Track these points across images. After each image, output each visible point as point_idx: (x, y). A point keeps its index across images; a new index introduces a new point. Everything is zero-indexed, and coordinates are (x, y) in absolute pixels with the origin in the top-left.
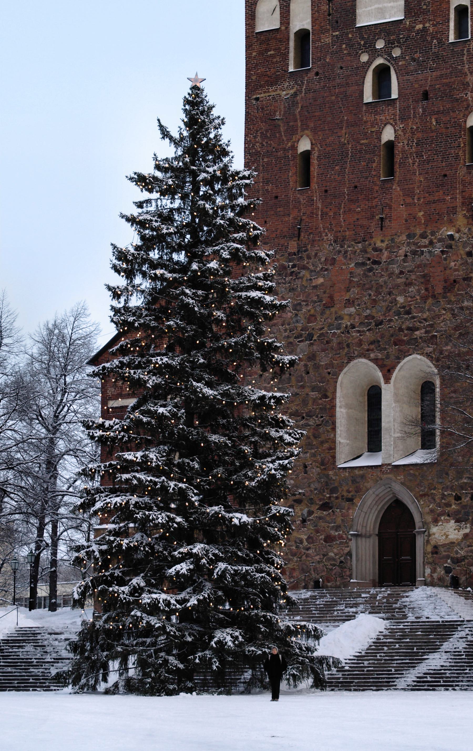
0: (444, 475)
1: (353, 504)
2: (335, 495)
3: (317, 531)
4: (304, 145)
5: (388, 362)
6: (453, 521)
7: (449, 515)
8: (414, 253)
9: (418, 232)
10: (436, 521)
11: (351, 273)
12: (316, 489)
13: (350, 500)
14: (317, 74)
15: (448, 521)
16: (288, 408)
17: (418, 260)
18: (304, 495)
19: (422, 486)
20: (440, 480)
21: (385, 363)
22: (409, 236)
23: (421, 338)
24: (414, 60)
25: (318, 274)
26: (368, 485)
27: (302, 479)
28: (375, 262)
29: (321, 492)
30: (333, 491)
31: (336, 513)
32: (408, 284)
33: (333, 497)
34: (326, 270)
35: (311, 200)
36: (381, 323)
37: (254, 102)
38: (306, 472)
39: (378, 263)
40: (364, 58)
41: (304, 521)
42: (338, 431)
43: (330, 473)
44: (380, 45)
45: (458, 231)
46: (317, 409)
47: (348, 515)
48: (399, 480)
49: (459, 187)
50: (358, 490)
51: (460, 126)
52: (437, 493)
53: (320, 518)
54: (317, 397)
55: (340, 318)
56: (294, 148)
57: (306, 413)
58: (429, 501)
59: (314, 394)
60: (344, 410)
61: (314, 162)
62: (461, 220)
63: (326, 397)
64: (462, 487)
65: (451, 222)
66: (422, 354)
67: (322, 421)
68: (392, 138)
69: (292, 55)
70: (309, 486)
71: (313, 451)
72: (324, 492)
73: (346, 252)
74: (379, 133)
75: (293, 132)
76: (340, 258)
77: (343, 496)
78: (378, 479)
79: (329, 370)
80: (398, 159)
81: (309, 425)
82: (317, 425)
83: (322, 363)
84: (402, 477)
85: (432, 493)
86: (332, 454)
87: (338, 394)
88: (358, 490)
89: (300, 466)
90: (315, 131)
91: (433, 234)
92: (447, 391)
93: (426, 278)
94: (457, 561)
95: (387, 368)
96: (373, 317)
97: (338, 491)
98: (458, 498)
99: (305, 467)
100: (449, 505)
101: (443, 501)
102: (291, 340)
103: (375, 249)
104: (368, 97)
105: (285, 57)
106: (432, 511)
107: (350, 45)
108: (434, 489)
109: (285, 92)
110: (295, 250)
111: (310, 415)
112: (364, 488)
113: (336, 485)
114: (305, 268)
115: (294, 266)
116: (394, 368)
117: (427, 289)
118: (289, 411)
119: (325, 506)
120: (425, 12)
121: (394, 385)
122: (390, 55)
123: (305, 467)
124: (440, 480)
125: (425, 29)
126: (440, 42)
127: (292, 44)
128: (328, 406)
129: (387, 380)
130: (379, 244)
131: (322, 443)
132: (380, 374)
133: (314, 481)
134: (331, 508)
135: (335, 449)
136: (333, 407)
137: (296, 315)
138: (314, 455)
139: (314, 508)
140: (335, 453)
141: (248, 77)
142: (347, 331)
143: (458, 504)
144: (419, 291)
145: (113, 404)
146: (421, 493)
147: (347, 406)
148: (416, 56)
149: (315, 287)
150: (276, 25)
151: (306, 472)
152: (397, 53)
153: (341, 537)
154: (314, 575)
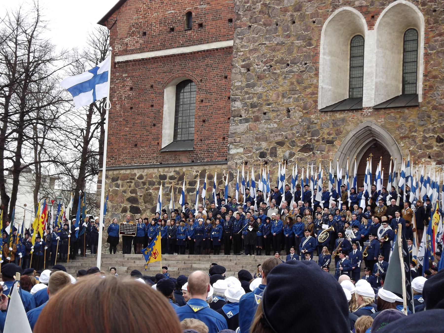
0: (426, 118)
1: (333, 146)
2: (316, 138)
6: (434, 163)
7: (430, 157)
12: (297, 132)
13: (331, 142)
15: (428, 163)
16: (274, 56)
18: (286, 138)
19: (402, 129)
20: (422, 123)
21: (369, 10)
26: (348, 128)
27: (285, 122)
31: (317, 155)
33: (314, 139)
38: (289, 116)
42: (320, 76)
43: (312, 116)
46: (301, 56)
47: (328, 157)
48: (380, 122)
50: (339, 133)
52: (419, 136)
54: (301, 45)
57: (291, 60)
58: (409, 143)
59: (298, 43)
60: (328, 58)
63: (310, 45)
67: (306, 68)
70: (292, 130)
71: (296, 96)
72: (305, 135)
77: (323, 139)
78: (359, 122)
79: (314, 19)
81: (293, 72)
82: (301, 72)
83: (308, 13)
84: (383, 120)
85: (413, 136)
86: (314, 99)
87: (322, 42)
88: (339, 133)
89: (283, 110)
92: (431, 34)
95: (370, 15)
97: (319, 134)
99: (289, 111)
100: (430, 147)
101: (424, 143)
108: (415, 131)
112: (344, 131)
113: (317, 128)
116: (378, 14)
118: (275, 59)
119: (306, 148)
121: (378, 31)
123: (289, 111)
124: (422, 123)
128: (312, 54)
129: (371, 25)
131: (305, 88)
133: (296, 125)
134: (312, 150)
135: (317, 94)
136: (317, 54)
139: (295, 150)
140: (317, 97)
143: (440, 146)
145: (119, 59)
146: (401, 135)
147: (331, 54)
151: (289, 116)
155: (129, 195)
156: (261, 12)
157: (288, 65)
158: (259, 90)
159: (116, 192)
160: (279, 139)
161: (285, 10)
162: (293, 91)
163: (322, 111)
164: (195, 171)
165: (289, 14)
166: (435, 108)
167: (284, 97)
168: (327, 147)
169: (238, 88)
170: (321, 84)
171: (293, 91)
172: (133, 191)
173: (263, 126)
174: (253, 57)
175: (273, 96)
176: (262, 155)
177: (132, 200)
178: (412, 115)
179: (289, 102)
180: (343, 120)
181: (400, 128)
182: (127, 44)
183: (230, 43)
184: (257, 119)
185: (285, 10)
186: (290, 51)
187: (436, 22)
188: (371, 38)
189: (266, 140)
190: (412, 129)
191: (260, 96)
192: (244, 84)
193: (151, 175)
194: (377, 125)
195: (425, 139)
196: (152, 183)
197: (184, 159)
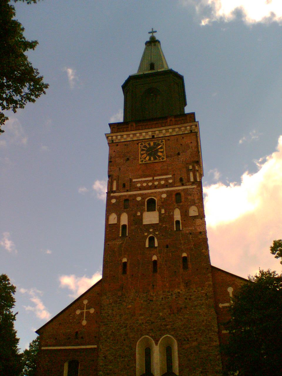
4: (125, 260)
8: (165, 298)
9: (167, 290)
11: (142, 304)
14: (129, 238)
22: (163, 292)
23: (169, 328)
24: (163, 235)
28: (150, 301)
34: (133, 302)
36: (153, 322)
37: (107, 245)
39: (152, 301)
45: (181, 291)
55: (138, 320)
56: (121, 260)
61: (128, 265)
62: (182, 287)
66: (170, 335)
68: (156, 259)
69: (121, 232)
73: (140, 296)
74: (151, 257)
80: (158, 266)
91: (172, 291)
96: (150, 320)
102: (119, 327)
103: (151, 296)
104: (147, 245)
105: (119, 232)
109: (118, 242)
110: (121, 295)
114: (124, 301)
115: (120, 300)
116: (159, 339)
117: (171, 311)
121: (159, 346)
122: (155, 233)
125: (166, 226)
126: (171, 230)
127: (121, 228)
129: (156, 344)
130: (152, 294)
132: (154, 342)
137: (121, 318)
141: (105, 237)
142: (140, 325)
144: (168, 311)
145: (43, 348)
147: (140, 354)
148: (163, 234)
149: (128, 309)
150: (115, 222)
152: (157, 233)
156: (111, 335)
157: (123, 358)
158: (111, 367)
165: (123, 336)
170: (137, 367)
182: (47, 342)
183: (96, 346)
187: (181, 344)
192: (104, 364)
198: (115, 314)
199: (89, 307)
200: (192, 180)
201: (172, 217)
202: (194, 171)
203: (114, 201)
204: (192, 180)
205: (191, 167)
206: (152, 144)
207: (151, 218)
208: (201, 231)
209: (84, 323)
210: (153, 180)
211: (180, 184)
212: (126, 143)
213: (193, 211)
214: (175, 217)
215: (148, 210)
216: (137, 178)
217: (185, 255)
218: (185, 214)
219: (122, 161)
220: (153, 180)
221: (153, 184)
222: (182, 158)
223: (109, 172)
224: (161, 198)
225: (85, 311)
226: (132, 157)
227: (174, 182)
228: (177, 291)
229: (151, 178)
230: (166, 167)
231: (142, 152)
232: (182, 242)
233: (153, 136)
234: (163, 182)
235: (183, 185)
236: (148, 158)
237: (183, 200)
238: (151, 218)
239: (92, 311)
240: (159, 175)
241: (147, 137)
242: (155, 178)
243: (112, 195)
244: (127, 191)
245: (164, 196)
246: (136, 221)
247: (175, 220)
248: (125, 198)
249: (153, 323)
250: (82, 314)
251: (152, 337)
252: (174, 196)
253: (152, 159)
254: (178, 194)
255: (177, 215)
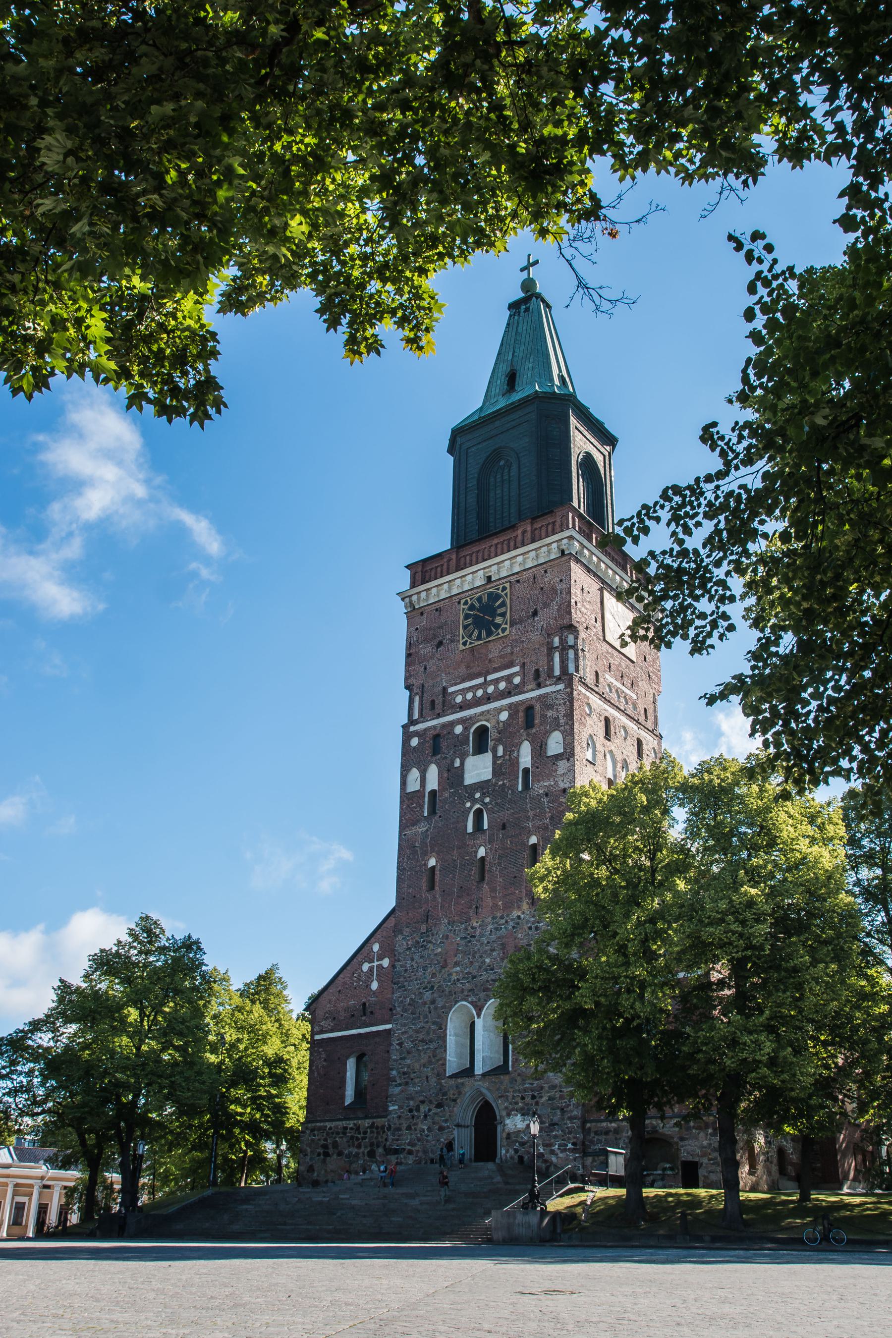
3: (434, 1123)
4: (432, 862)
5: (479, 1004)
8: (496, 929)
9: (499, 915)
10: (509, 1115)
17: (498, 934)
22: (493, 918)
25: (438, 946)
29: (437, 1095)
30: (445, 1094)
32: (493, 950)
35: (434, 897)
36: (474, 977)
40: (468, 805)
41: (426, 1116)
44: (478, 795)
49: (524, 884)
51: (524, 844)
52: (510, 1095)
53: (436, 1114)
55: (451, 974)
56: (426, 864)
60: (453, 1038)
61: (437, 872)
62: (525, 906)
64: (525, 1090)
65: (519, 907)
69: (426, 806)
74: (476, 852)
75: (425, 855)
76: (451, 934)
80: (487, 868)
88: (460, 1093)
90: (438, 854)
93: (503, 946)
94: (523, 1144)
98: (523, 1098)
100: (517, 1103)
104: (470, 829)
105: (422, 807)
106: (506, 1108)
107: (459, 797)
109: (421, 828)
111: (431, 1041)
114: (430, 942)
119: (439, 1105)
120: (504, 774)
127: (426, 799)
129: (479, 1016)
130: (475, 924)
138: (433, 1069)
145: (317, 1037)
147: (456, 1035)
150: (418, 788)
152: (487, 800)
153: (448, 1127)
154: (431, 1155)
155: (322, 1142)
158: (408, 1061)
159: (313, 1140)
160: (422, 1098)
161: (425, 1003)
162: (430, 1062)
163: (450, 1077)
164: (367, 1123)
166: (519, 1075)
167: (424, 1066)
168: (452, 1104)
169: (395, 1060)
171: (430, 1062)
172: (326, 1140)
173: (412, 1089)
174: (404, 1037)
175: (417, 1066)
176: (411, 1111)
177: (325, 1146)
178: (505, 1079)
179: (428, 1071)
180: (463, 1084)
181: (498, 1089)
183: (389, 1026)
184: (407, 1083)
185: (425, 1003)
186: (428, 1033)
188: (479, 1024)
189: (412, 1099)
190: (506, 1091)
191: (409, 1066)
193: (336, 1127)
194: (484, 1087)
195: (514, 1097)
196: (338, 1133)
197: (360, 1115)
198: (415, 966)
199: (380, 958)
200: (557, 672)
201: (515, 762)
202: (564, 648)
203: (415, 742)
204: (557, 672)
205: (556, 641)
206: (485, 599)
207: (478, 769)
208: (566, 786)
209: (375, 986)
210: (485, 684)
211: (533, 685)
212: (437, 606)
213: (555, 744)
214: (521, 760)
215: (474, 754)
216: (456, 684)
217: (533, 840)
218: (539, 750)
219: (430, 649)
220: (485, 684)
221: (485, 692)
222: (541, 620)
223: (406, 679)
224: (498, 722)
225: (376, 963)
226: (448, 637)
227: (523, 682)
228: (515, 913)
229: (481, 680)
230: (509, 650)
231: (467, 622)
232: (531, 813)
233: (489, 578)
234: (502, 685)
235: (539, 686)
236: (476, 633)
237: (537, 721)
238: (478, 769)
239: (386, 963)
240: (496, 670)
241: (478, 583)
242: (489, 678)
243: (412, 729)
244: (439, 716)
245: (504, 716)
246: (452, 777)
247: (522, 767)
248: (433, 732)
249: (474, 977)
250: (371, 969)
251: (471, 1003)
252: (521, 714)
253: (484, 634)
254: (529, 710)
255: (525, 758)
